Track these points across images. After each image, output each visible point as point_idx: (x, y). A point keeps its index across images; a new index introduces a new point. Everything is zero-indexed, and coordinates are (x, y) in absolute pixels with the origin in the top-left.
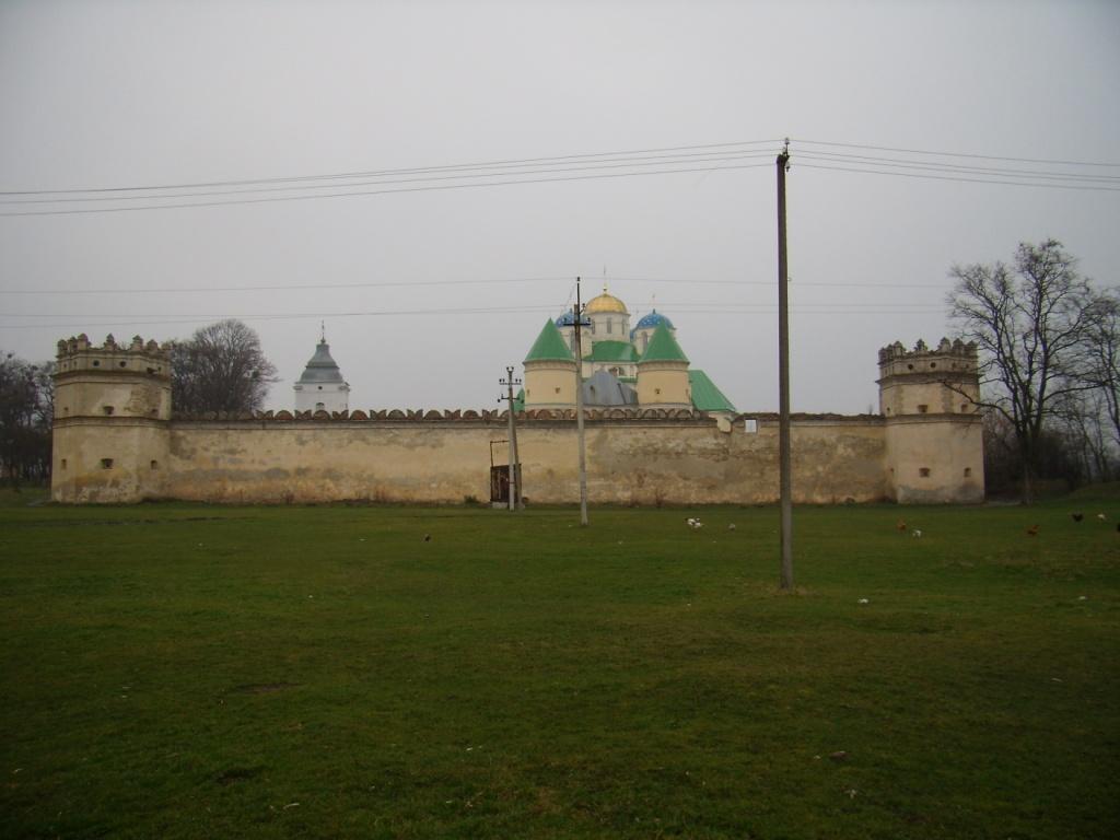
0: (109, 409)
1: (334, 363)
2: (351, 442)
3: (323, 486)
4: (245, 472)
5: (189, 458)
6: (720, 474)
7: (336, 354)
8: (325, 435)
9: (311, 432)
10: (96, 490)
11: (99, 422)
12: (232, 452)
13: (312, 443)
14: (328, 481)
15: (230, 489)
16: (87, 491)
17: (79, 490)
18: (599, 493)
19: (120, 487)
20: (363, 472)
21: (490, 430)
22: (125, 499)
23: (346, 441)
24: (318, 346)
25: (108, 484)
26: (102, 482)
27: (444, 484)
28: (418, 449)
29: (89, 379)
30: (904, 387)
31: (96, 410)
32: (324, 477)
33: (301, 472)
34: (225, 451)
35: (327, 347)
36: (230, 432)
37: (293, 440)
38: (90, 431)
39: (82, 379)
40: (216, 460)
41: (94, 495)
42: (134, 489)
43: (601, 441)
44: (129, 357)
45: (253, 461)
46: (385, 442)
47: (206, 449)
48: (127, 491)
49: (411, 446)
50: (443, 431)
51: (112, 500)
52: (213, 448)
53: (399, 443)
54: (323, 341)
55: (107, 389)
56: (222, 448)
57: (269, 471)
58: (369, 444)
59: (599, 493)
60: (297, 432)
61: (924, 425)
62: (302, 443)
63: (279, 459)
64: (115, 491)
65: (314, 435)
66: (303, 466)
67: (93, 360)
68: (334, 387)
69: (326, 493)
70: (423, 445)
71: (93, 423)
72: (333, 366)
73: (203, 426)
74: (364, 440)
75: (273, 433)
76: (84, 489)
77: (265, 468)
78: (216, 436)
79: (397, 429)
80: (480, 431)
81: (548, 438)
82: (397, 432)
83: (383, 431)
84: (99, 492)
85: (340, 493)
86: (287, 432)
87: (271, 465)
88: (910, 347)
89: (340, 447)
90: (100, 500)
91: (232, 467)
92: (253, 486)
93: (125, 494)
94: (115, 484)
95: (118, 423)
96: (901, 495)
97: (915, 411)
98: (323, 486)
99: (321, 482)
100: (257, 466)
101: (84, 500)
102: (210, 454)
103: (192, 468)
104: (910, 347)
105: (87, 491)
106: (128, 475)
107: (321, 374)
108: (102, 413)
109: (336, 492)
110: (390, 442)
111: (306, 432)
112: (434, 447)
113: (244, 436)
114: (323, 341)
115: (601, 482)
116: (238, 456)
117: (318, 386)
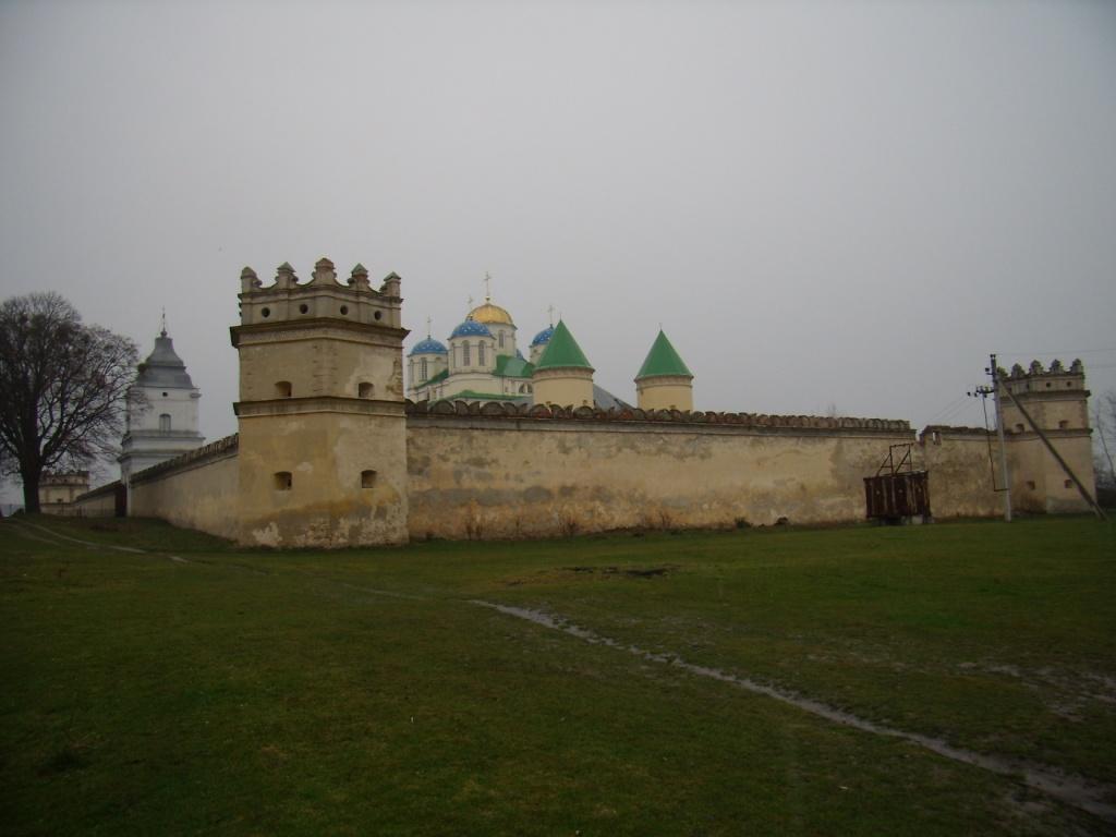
0: (364, 387)
1: (181, 362)
2: (619, 450)
3: (592, 511)
4: (498, 493)
5: (420, 472)
6: (271, 528)
7: (181, 350)
8: (591, 440)
9: (575, 436)
10: (357, 523)
11: (356, 409)
12: (479, 463)
13: (576, 450)
14: (598, 503)
15: (478, 519)
16: (345, 525)
17: (334, 524)
18: (841, 511)
19: (388, 518)
20: (635, 490)
21: (751, 438)
22: (394, 537)
23: (614, 449)
24: (158, 340)
25: (373, 513)
26: (361, 510)
27: (715, 505)
28: (688, 460)
29: (340, 334)
30: (1045, 404)
31: (350, 390)
32: (592, 499)
33: (567, 491)
34: (468, 462)
35: (170, 341)
36: (476, 433)
37: (554, 446)
38: (345, 423)
39: (331, 334)
40: (458, 475)
41: (355, 532)
42: (405, 519)
43: (839, 451)
44: (387, 305)
45: (507, 477)
46: (654, 449)
47: (444, 459)
48: (397, 524)
49: (681, 457)
50: (710, 438)
51: (379, 540)
52: (453, 457)
53: (669, 453)
54: (164, 334)
55: (362, 354)
56: (466, 456)
57: (528, 491)
58: (639, 453)
59: (841, 511)
60: (558, 435)
61: (1066, 440)
62: (566, 451)
63: (538, 473)
64: (381, 524)
65: (579, 440)
66: (569, 483)
67: (341, 304)
68: (185, 394)
69: (597, 520)
70: (693, 455)
71: (349, 410)
72: (179, 367)
73: (439, 423)
74: (633, 447)
75: (531, 436)
76: (342, 521)
77: (523, 487)
78: (456, 439)
79: (665, 433)
80: (744, 439)
81: (798, 448)
82: (666, 438)
83: (653, 436)
84: (361, 526)
85: (613, 519)
86: (547, 435)
87: (530, 482)
88: (1046, 366)
89: (610, 457)
90: (363, 541)
91: (480, 486)
92: (510, 513)
93: (394, 529)
94: (381, 513)
95: (380, 411)
96: (1049, 506)
97: (1057, 427)
98: (592, 511)
99: (590, 505)
100: (512, 484)
101: (341, 540)
102: (449, 466)
103: (427, 486)
104: (1046, 366)
105: (345, 525)
106: (396, 499)
107: (164, 375)
108: (355, 394)
109: (607, 518)
110: (660, 450)
111: (569, 436)
112: (703, 457)
113: (493, 440)
114: (164, 334)
115: (838, 499)
116: (487, 470)
117: (162, 391)
